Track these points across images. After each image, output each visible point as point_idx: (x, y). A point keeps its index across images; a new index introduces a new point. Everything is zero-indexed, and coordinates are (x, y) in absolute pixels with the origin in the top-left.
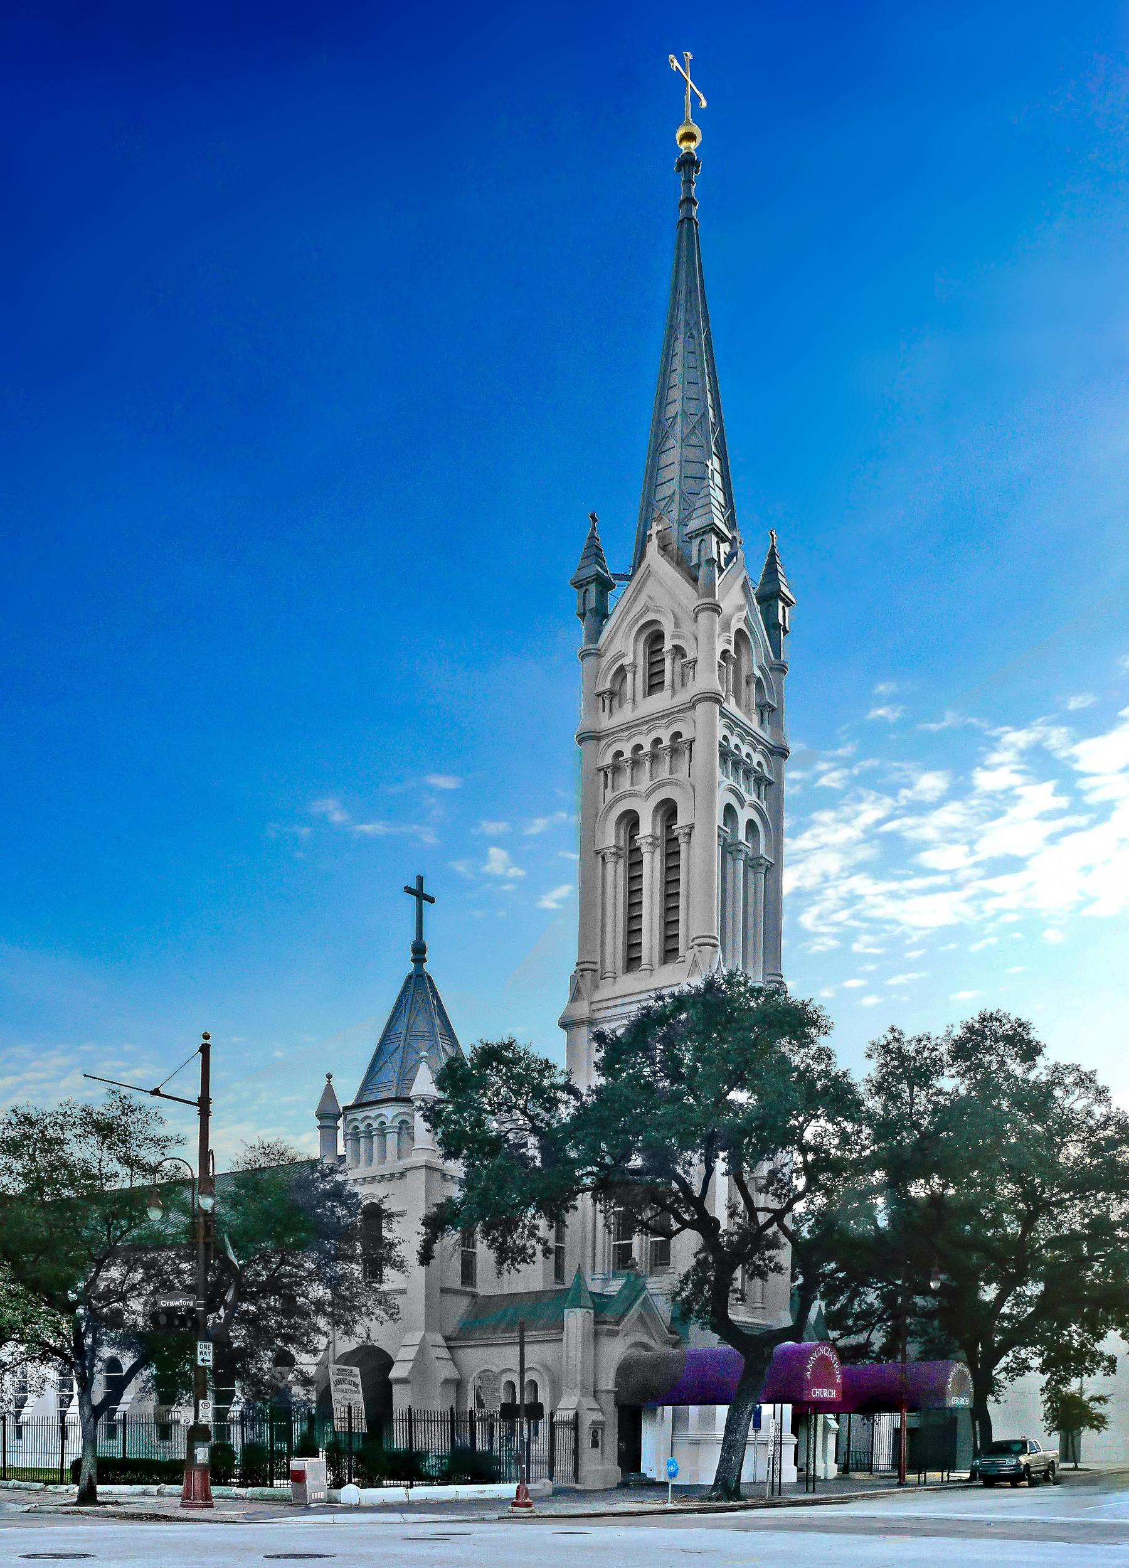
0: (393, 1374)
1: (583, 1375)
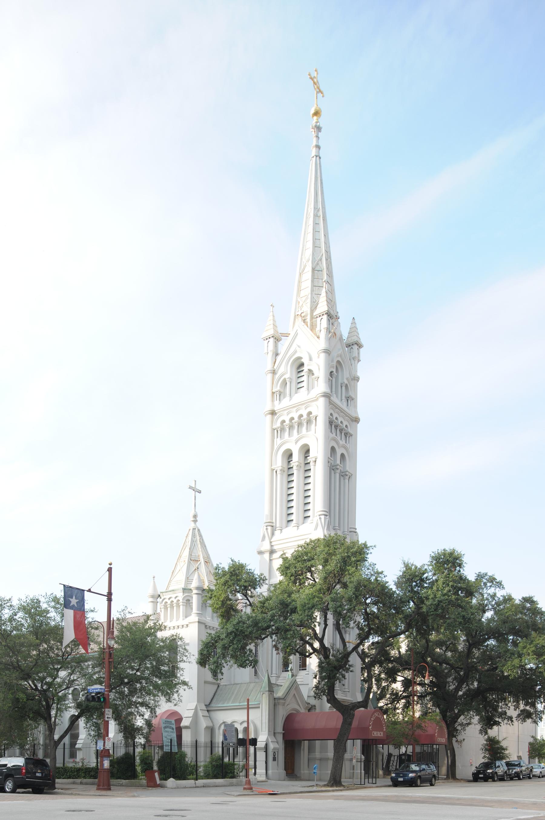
0: (77, 746)
1: (225, 737)
